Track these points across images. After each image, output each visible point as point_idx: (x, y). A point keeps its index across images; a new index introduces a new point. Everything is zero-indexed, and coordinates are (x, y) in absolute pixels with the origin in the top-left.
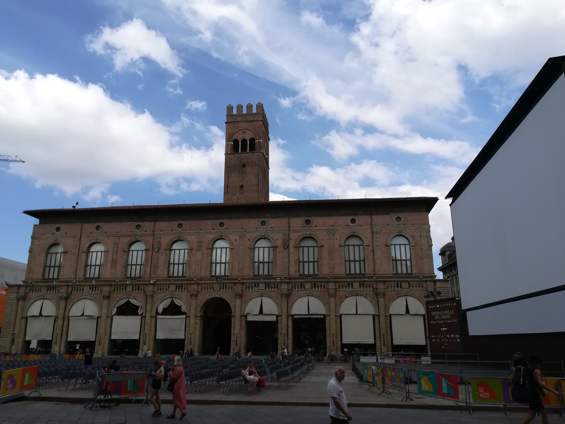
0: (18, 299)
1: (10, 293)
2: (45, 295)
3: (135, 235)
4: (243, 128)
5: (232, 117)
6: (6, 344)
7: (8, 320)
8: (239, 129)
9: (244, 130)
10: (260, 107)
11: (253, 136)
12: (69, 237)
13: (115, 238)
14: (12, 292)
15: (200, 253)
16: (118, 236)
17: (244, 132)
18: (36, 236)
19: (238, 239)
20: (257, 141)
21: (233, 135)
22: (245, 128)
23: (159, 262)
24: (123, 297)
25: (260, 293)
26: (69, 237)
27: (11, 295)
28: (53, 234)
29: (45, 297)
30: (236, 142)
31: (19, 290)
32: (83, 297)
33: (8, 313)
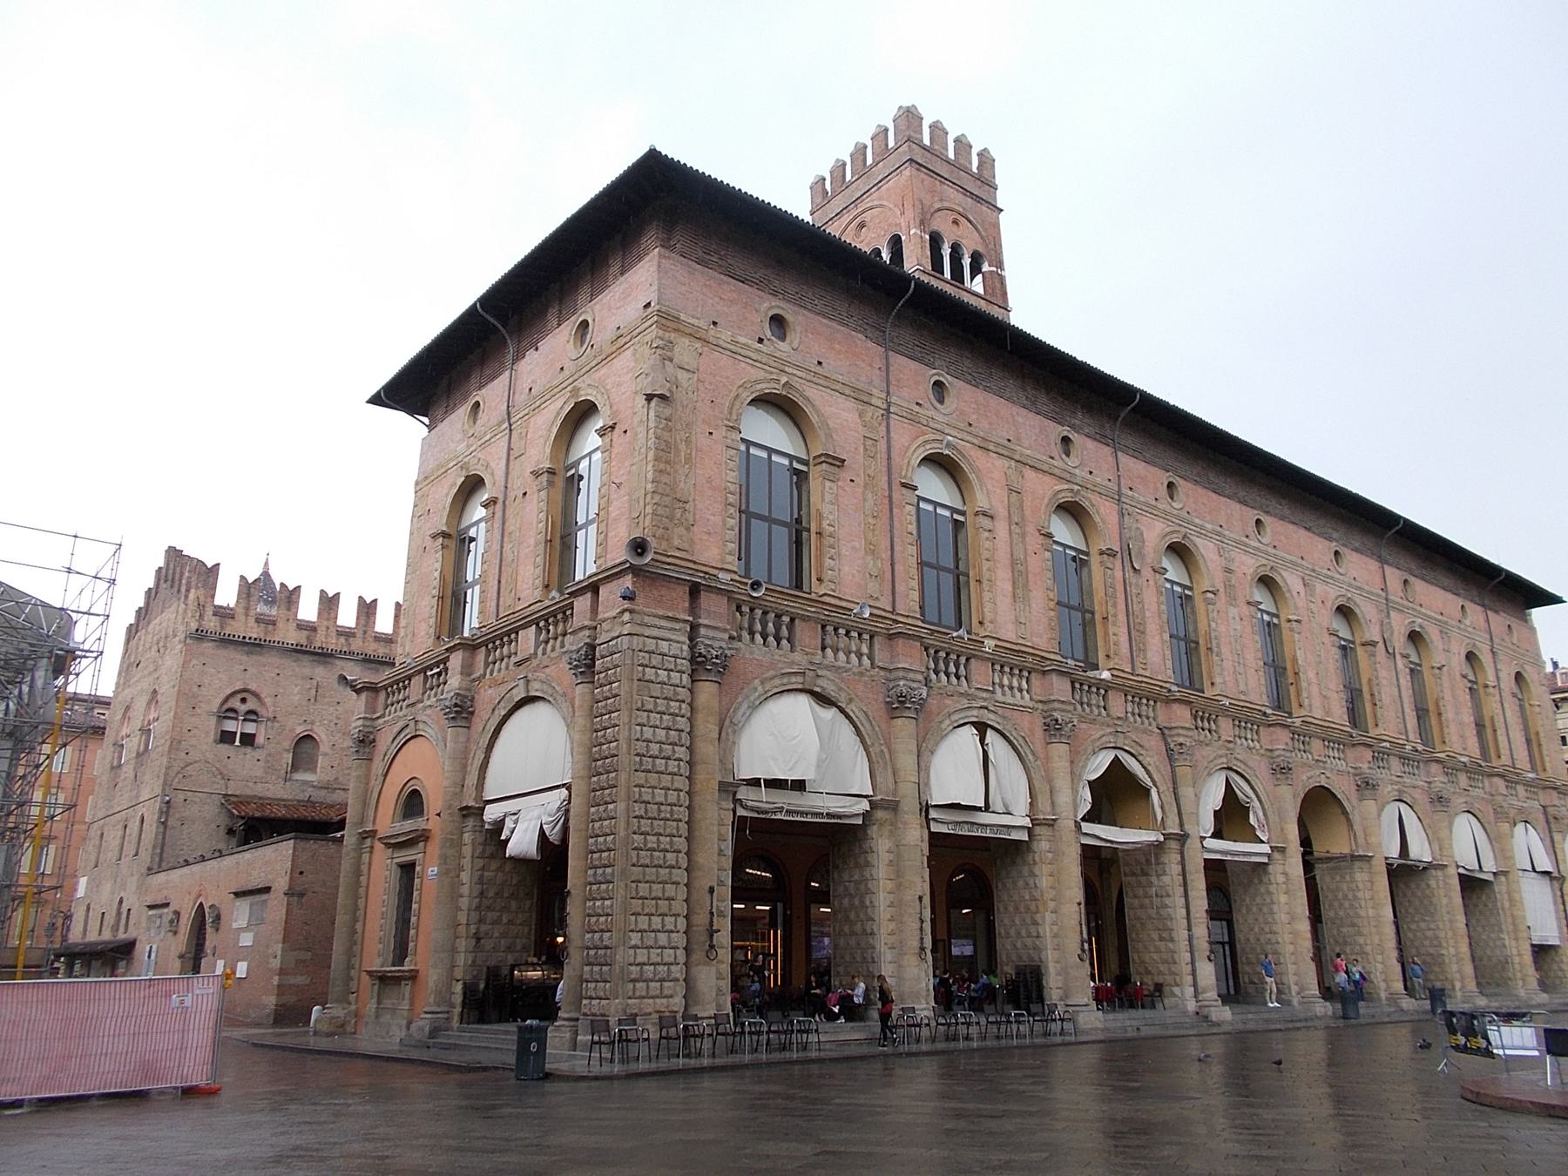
0: (698, 663)
1: (647, 619)
2: (820, 672)
3: (1067, 476)
4: (957, 208)
5: (923, 151)
6: (669, 955)
7: (659, 795)
8: (946, 204)
9: (959, 217)
10: (986, 159)
11: (981, 249)
12: (838, 387)
13: (1006, 463)
14: (668, 618)
15: (1233, 612)
16: (1017, 457)
17: (955, 222)
18: (683, 317)
19: (1301, 588)
20: (995, 269)
21: (932, 215)
22: (961, 210)
23: (1148, 614)
24: (1104, 739)
25: (1396, 787)
26: (838, 387)
27: (655, 632)
28: (761, 341)
29: (820, 682)
30: (935, 241)
31: (694, 608)
32: (975, 712)
33: (655, 749)
